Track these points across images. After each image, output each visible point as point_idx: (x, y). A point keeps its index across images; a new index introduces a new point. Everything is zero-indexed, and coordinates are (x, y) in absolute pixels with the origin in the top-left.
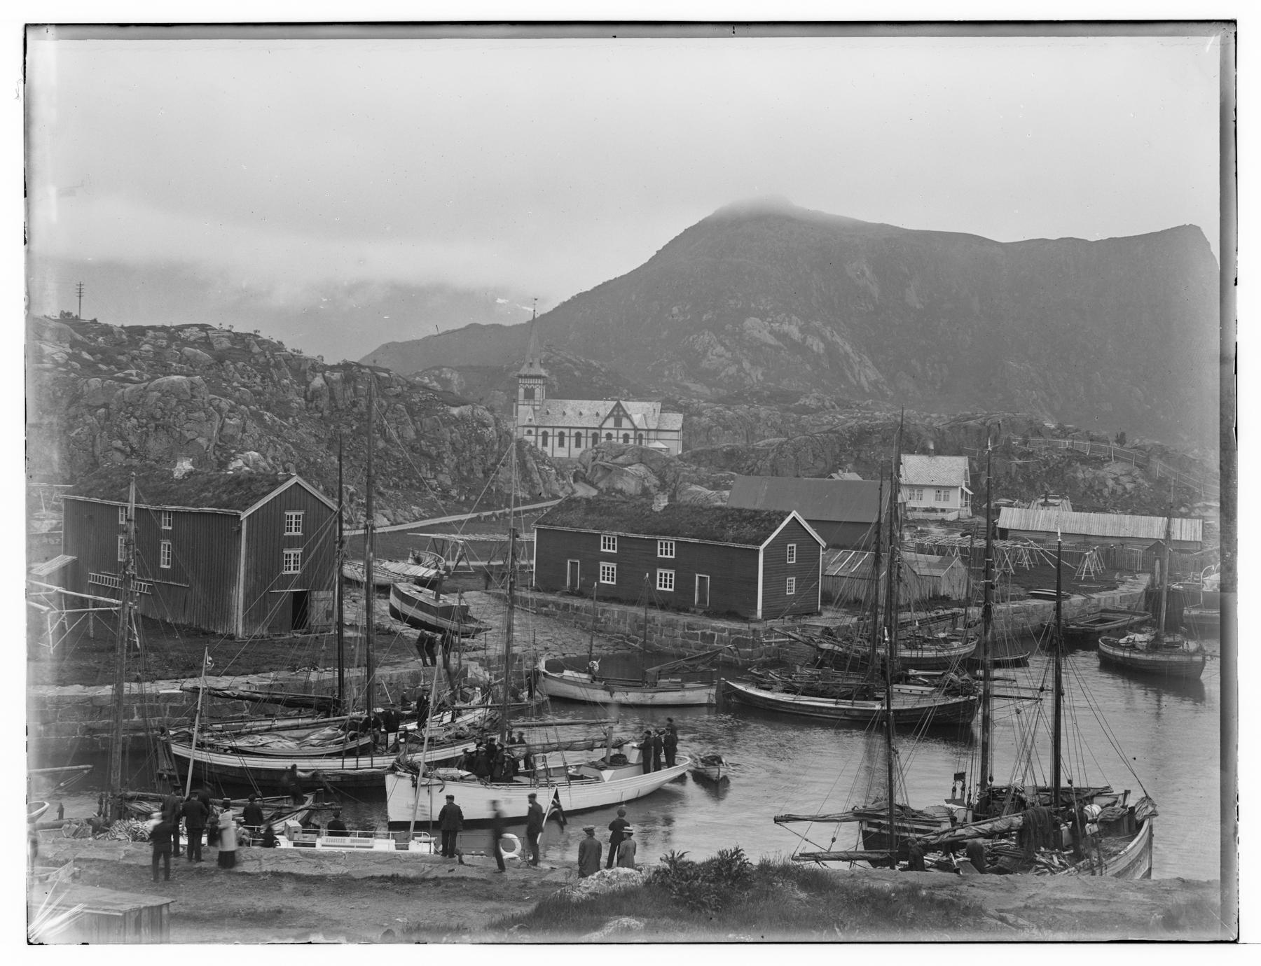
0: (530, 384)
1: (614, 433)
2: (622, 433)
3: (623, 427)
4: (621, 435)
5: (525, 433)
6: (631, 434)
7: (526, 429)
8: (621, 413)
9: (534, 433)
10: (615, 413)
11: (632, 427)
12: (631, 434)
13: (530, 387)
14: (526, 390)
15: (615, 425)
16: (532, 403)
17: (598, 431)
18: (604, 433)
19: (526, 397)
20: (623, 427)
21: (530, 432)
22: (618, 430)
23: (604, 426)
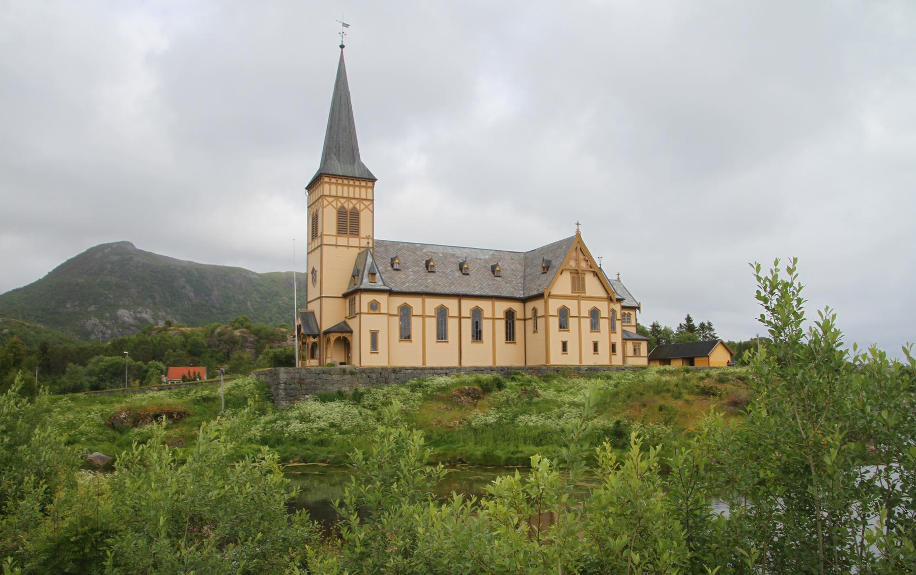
0: (349, 199)
1: (572, 305)
2: (587, 306)
3: (588, 294)
4: (585, 312)
5: (365, 308)
6: (604, 308)
7: (365, 300)
8: (583, 265)
9: (384, 309)
11: (604, 295)
12: (604, 308)
13: (349, 206)
14: (342, 213)
15: (574, 289)
16: (354, 241)
17: (516, 307)
18: (554, 306)
19: (342, 230)
20: (588, 293)
21: (374, 306)
22: (578, 299)
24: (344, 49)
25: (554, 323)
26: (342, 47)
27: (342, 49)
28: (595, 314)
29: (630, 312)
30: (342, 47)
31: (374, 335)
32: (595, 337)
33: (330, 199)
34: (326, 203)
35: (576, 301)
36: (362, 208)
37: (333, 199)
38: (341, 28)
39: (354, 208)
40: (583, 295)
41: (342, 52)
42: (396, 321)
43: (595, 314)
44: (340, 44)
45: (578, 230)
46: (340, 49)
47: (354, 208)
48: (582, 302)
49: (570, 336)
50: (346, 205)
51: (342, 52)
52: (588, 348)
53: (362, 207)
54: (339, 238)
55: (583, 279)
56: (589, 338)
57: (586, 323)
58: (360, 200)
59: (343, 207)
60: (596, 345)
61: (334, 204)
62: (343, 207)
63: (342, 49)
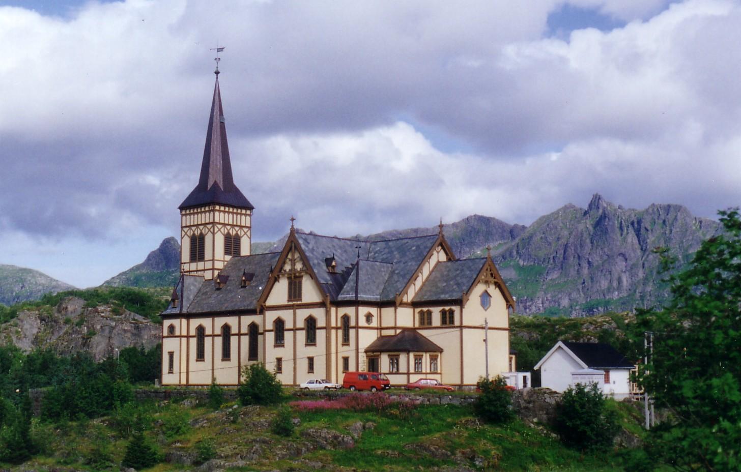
0: (197, 226)
1: (287, 316)
4: (301, 324)
10: (287, 267)
13: (197, 232)
15: (290, 298)
23: (270, 302)
24: (219, 75)
25: (270, 337)
26: (217, 73)
27: (217, 76)
28: (311, 324)
29: (453, 308)
30: (217, 73)
31: (171, 354)
32: (311, 351)
33: (186, 230)
34: (183, 233)
35: (292, 311)
36: (206, 232)
37: (188, 228)
38: (215, 54)
39: (201, 233)
40: (299, 302)
41: (217, 78)
42: (193, 342)
43: (311, 324)
44: (215, 70)
45: (292, 226)
46: (215, 75)
47: (201, 233)
48: (298, 311)
49: (285, 353)
50: (196, 232)
51: (217, 78)
52: (303, 365)
53: (207, 230)
54: (191, 264)
55: (300, 283)
56: (304, 351)
57: (302, 336)
58: (205, 224)
59: (194, 234)
60: (311, 360)
61: (188, 233)
62: (194, 234)
63: (217, 76)
